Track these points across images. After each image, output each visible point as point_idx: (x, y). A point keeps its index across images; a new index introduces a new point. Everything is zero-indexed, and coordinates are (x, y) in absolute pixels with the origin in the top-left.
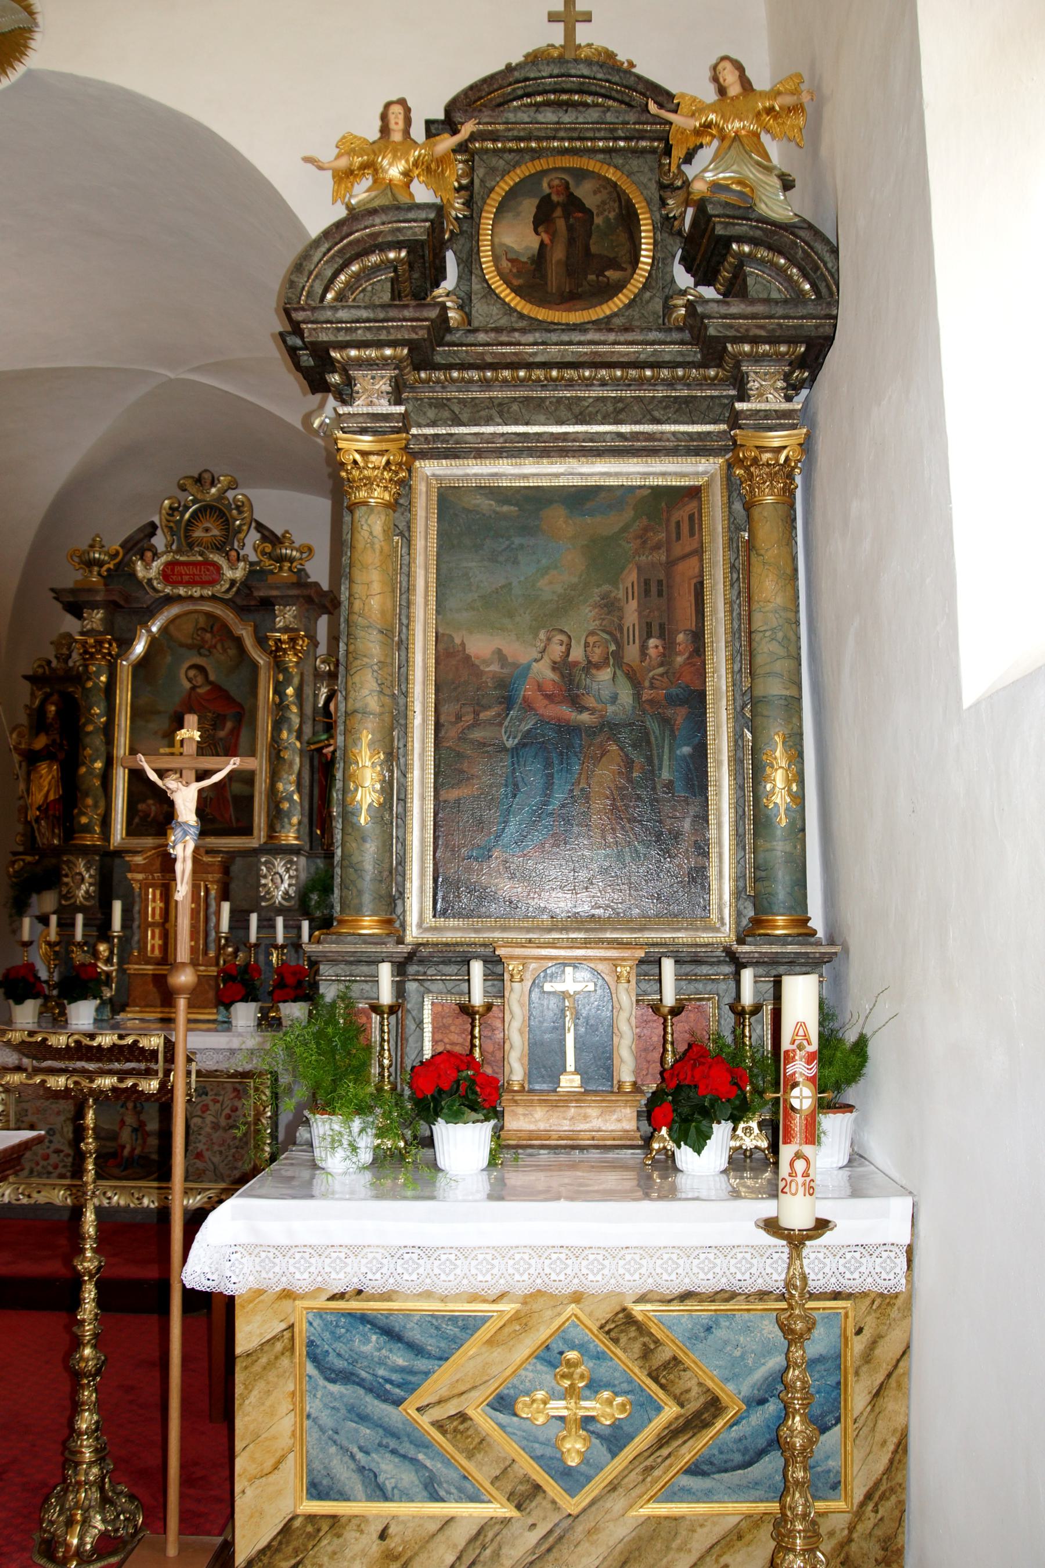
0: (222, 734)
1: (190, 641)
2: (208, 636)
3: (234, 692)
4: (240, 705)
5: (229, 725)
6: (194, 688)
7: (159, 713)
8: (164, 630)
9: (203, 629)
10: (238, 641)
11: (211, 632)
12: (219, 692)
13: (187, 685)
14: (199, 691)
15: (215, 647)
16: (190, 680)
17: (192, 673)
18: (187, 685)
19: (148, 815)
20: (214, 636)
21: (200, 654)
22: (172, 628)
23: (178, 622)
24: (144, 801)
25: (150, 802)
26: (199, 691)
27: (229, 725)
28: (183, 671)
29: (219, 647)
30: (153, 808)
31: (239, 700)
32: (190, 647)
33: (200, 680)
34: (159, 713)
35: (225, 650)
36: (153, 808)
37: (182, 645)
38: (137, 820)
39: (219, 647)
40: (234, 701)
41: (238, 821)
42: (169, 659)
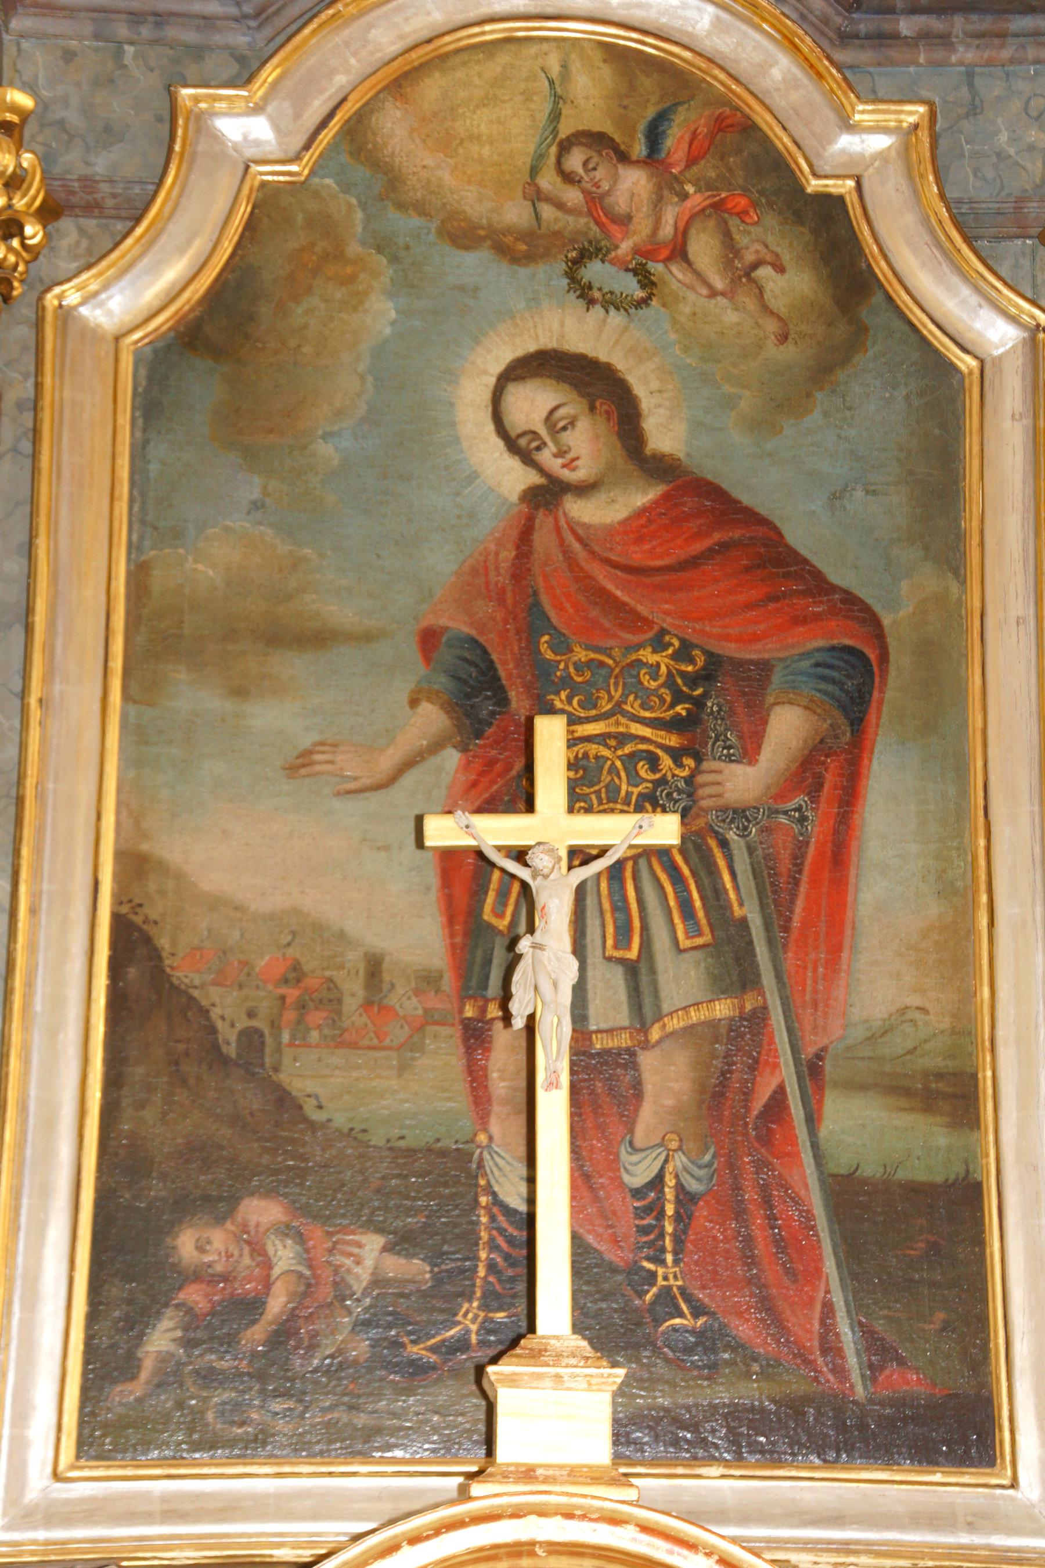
0: (741, 782)
1: (515, 214)
2: (632, 185)
3: (805, 529)
4: (853, 607)
5: (787, 728)
6: (547, 494)
7: (317, 638)
8: (353, 137)
9: (596, 140)
10: (830, 229)
11: (653, 158)
12: (710, 525)
13: (511, 478)
14: (583, 511)
15: (679, 251)
16: (519, 446)
17: (532, 404)
18: (511, 478)
19: (251, 1307)
20: (668, 185)
21: (585, 294)
22: (394, 127)
23: (431, 89)
24: (219, 1205)
25: (262, 1212)
26: (583, 511)
27: (787, 728)
28: (473, 394)
29: (703, 248)
30: (284, 1256)
31: (834, 576)
32: (518, 249)
33: (586, 446)
34: (317, 638)
35: (743, 276)
36: (284, 1256)
37: (463, 234)
38: (162, 1339)
39: (703, 248)
40: (818, 584)
41: (879, 1351)
42: (381, 314)
